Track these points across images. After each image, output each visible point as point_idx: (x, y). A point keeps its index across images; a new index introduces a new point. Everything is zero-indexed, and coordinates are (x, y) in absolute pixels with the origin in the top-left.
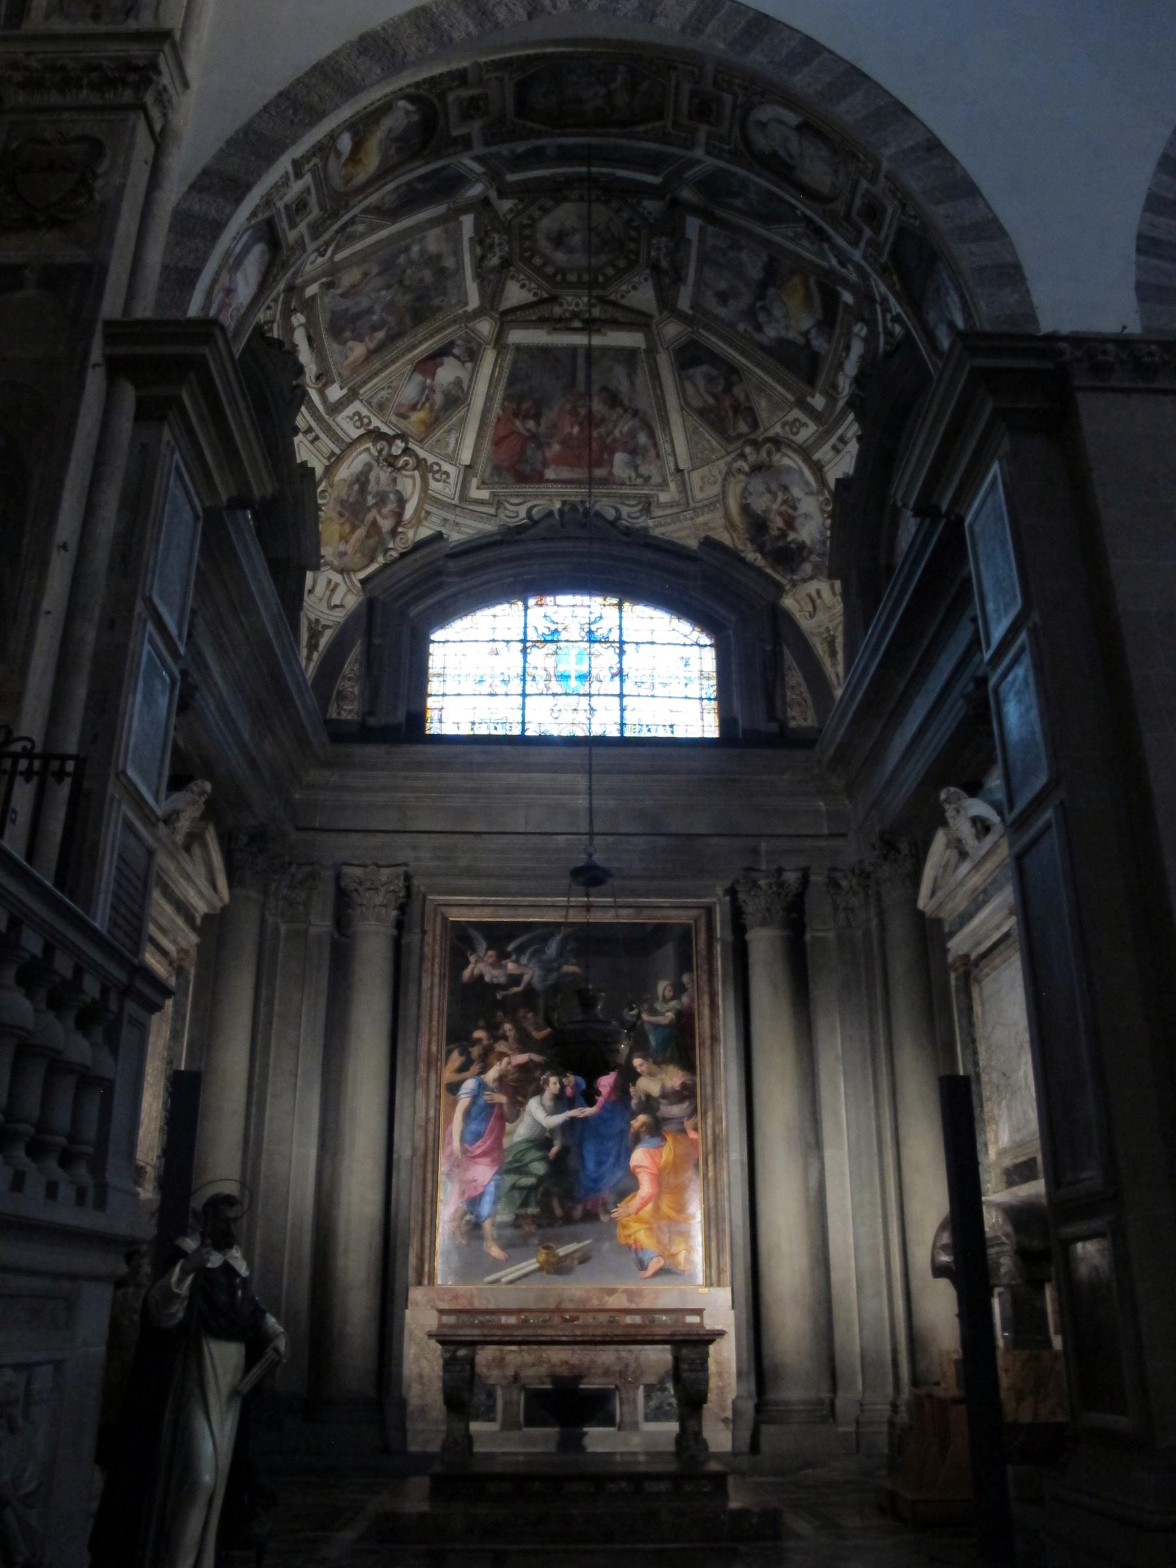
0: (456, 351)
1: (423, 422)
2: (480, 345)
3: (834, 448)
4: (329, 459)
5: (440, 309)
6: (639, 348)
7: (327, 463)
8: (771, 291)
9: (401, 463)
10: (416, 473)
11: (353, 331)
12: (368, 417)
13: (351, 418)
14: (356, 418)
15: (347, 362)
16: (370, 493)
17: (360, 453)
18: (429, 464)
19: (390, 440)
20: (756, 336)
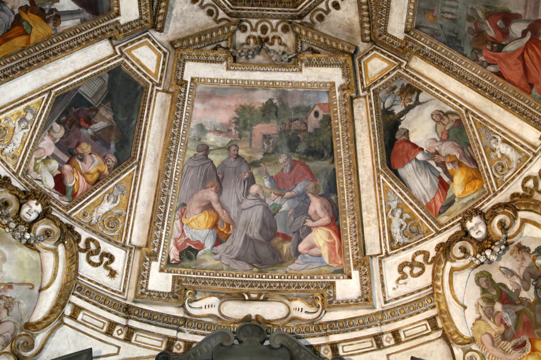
0: (398, 110)
1: (468, 181)
2: (399, 76)
4: (435, 328)
5: (327, 120)
7: (439, 333)
9: (498, 232)
10: (522, 214)
11: (286, 238)
12: (416, 254)
13: (404, 276)
14: (407, 270)
15: (326, 259)
16: (518, 291)
17: (451, 282)
18: (521, 191)
19: (465, 234)
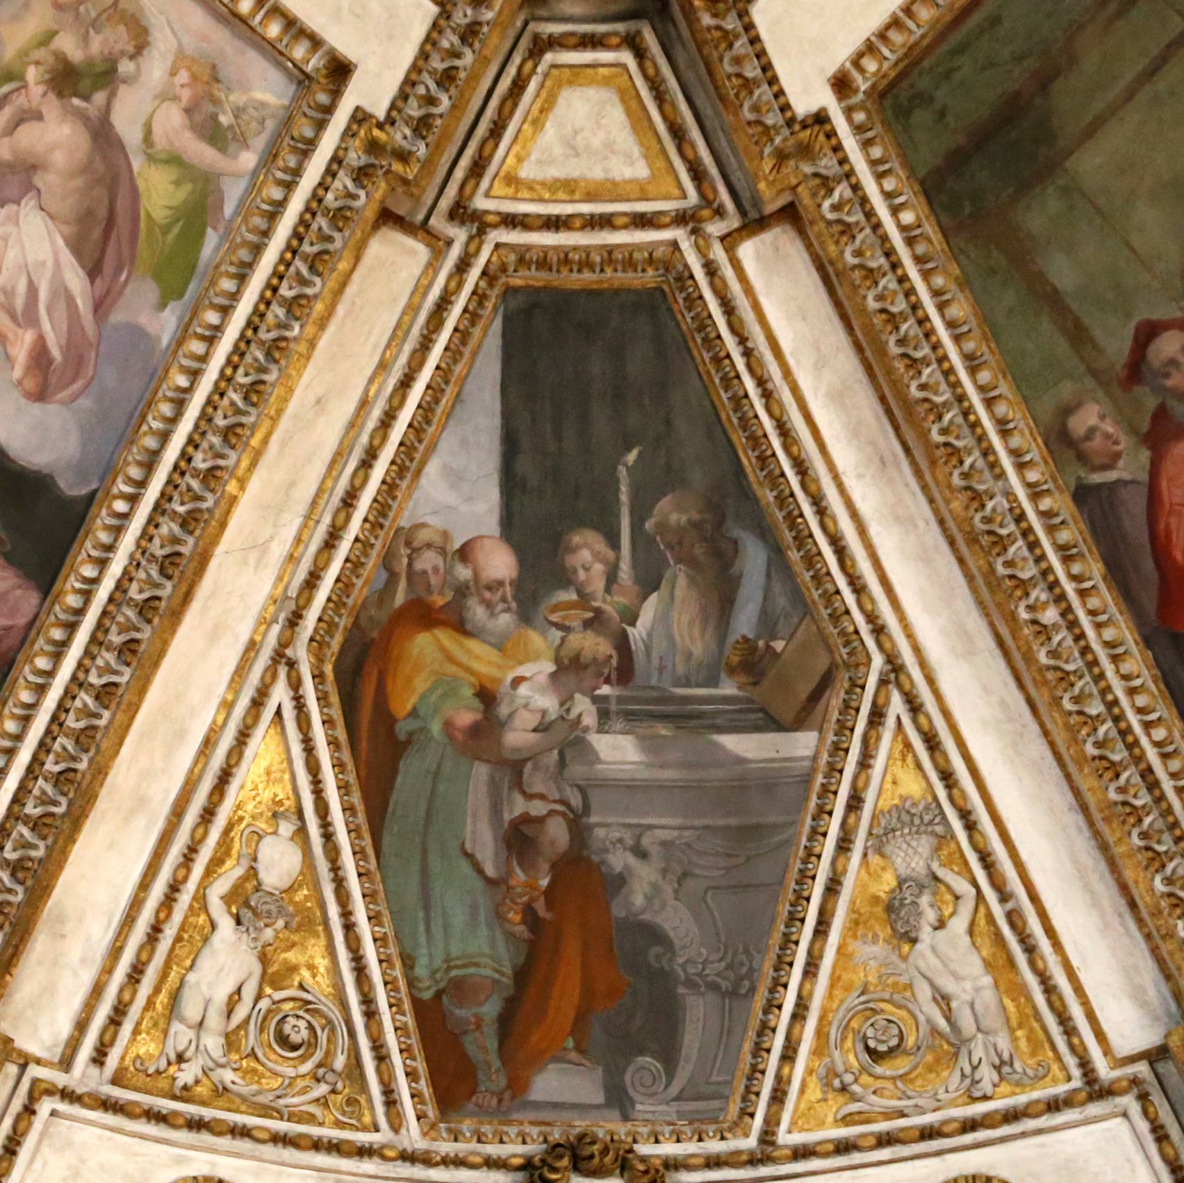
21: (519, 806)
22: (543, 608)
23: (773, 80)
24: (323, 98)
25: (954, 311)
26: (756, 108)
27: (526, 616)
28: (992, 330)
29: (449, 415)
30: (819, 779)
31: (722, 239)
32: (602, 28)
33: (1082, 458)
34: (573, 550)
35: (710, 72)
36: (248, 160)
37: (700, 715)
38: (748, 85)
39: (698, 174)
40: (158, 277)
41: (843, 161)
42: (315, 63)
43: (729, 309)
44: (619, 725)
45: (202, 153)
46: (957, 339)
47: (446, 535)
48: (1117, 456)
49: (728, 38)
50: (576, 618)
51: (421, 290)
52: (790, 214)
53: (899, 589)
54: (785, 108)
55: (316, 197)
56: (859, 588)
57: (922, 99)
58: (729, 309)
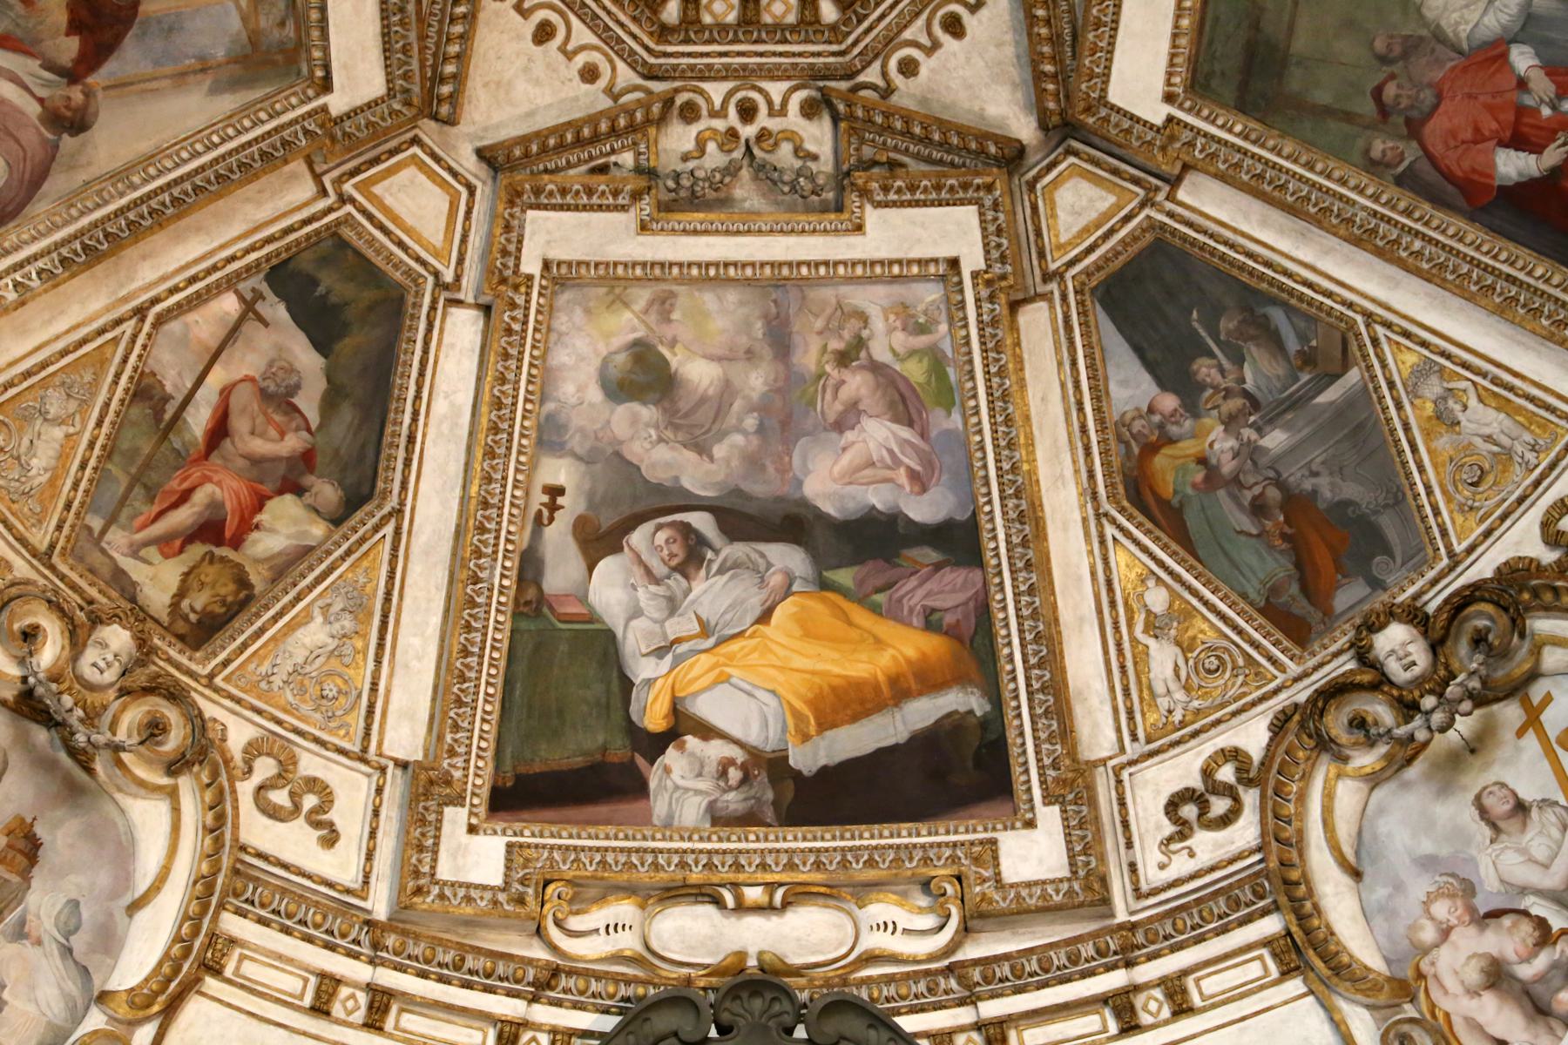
3: (329, 984)
6: (326, 86)
8: (786, 558)
20: (558, 537)
21: (1248, 496)
22: (1201, 405)
23: (1138, 120)
24: (955, 279)
25: (1287, 151)
26: (1139, 138)
27: (1196, 415)
28: (1308, 143)
29: (1104, 360)
30: (1371, 386)
31: (1167, 199)
32: (1052, 157)
33: (1388, 166)
34: (1196, 373)
35: (1108, 140)
36: (943, 328)
37: (1300, 398)
38: (1128, 131)
39: (1136, 181)
40: (939, 404)
41: (1192, 128)
42: (942, 269)
43: (1190, 224)
44: (1268, 429)
45: (922, 341)
46: (1296, 161)
47: (1137, 409)
48: (1402, 153)
49: (1106, 120)
50: (1218, 399)
51: (1053, 320)
52: (1186, 168)
53: (1348, 281)
54: (1152, 126)
55: (980, 322)
56: (1329, 294)
57: (1210, 75)
58: (1190, 224)
